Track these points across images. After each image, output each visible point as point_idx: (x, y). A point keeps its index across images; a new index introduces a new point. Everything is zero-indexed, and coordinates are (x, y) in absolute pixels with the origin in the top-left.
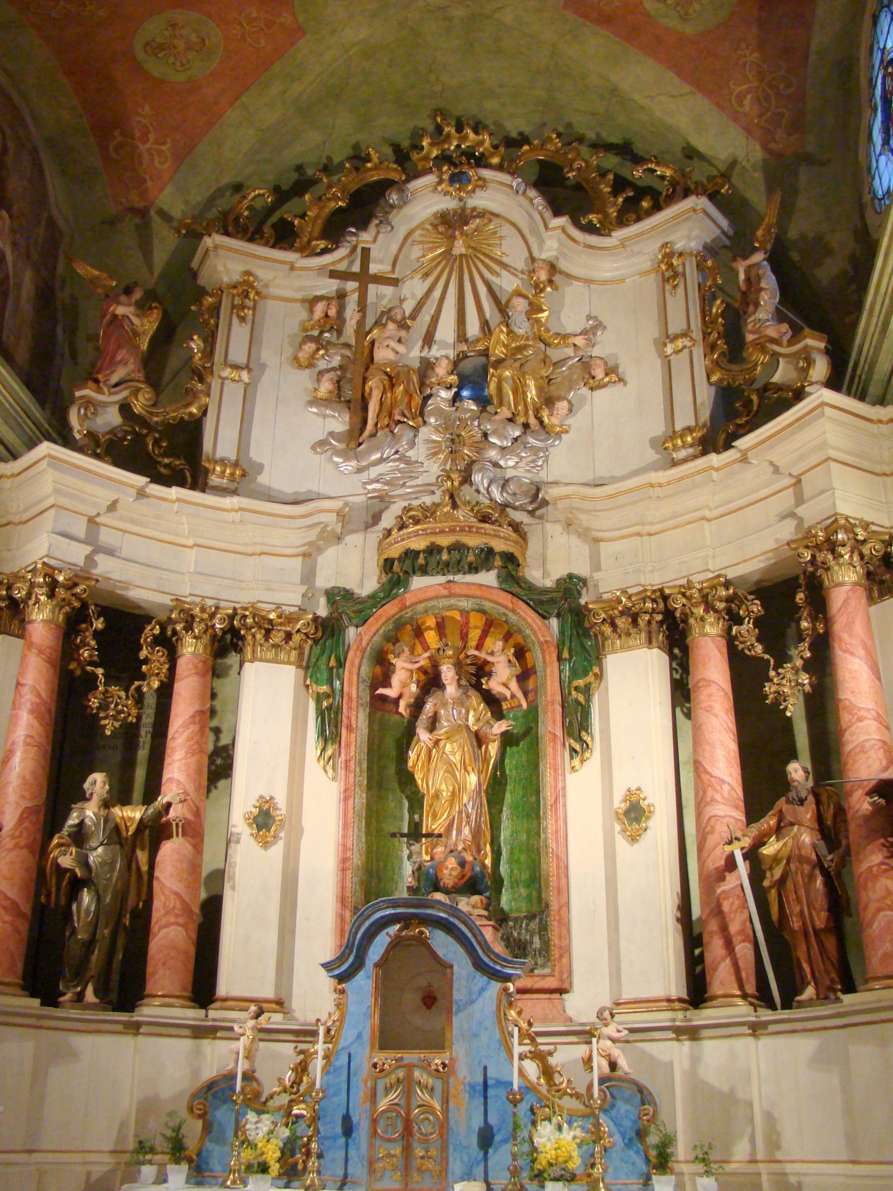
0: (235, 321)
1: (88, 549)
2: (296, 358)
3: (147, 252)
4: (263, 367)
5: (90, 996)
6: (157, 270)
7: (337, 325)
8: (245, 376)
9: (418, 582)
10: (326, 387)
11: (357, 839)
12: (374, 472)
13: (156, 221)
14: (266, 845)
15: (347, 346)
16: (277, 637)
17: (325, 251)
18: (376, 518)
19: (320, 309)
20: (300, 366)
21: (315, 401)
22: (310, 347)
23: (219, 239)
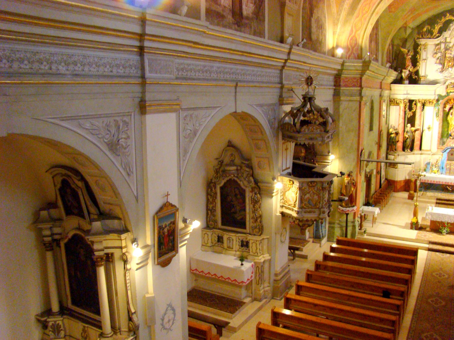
0: (424, 51)
1: (407, 95)
2: (433, 56)
3: (406, 33)
4: (428, 58)
5: (409, 150)
6: (407, 36)
7: (439, 49)
8: (426, 61)
9: (451, 94)
10: (438, 61)
11: (441, 130)
12: (445, 75)
13: (408, 28)
14: (429, 131)
15: (441, 52)
16: (431, 103)
17: (438, 37)
18: (445, 83)
19: (437, 47)
20: (434, 58)
21: (436, 63)
22: (435, 55)
23: (423, 40)
